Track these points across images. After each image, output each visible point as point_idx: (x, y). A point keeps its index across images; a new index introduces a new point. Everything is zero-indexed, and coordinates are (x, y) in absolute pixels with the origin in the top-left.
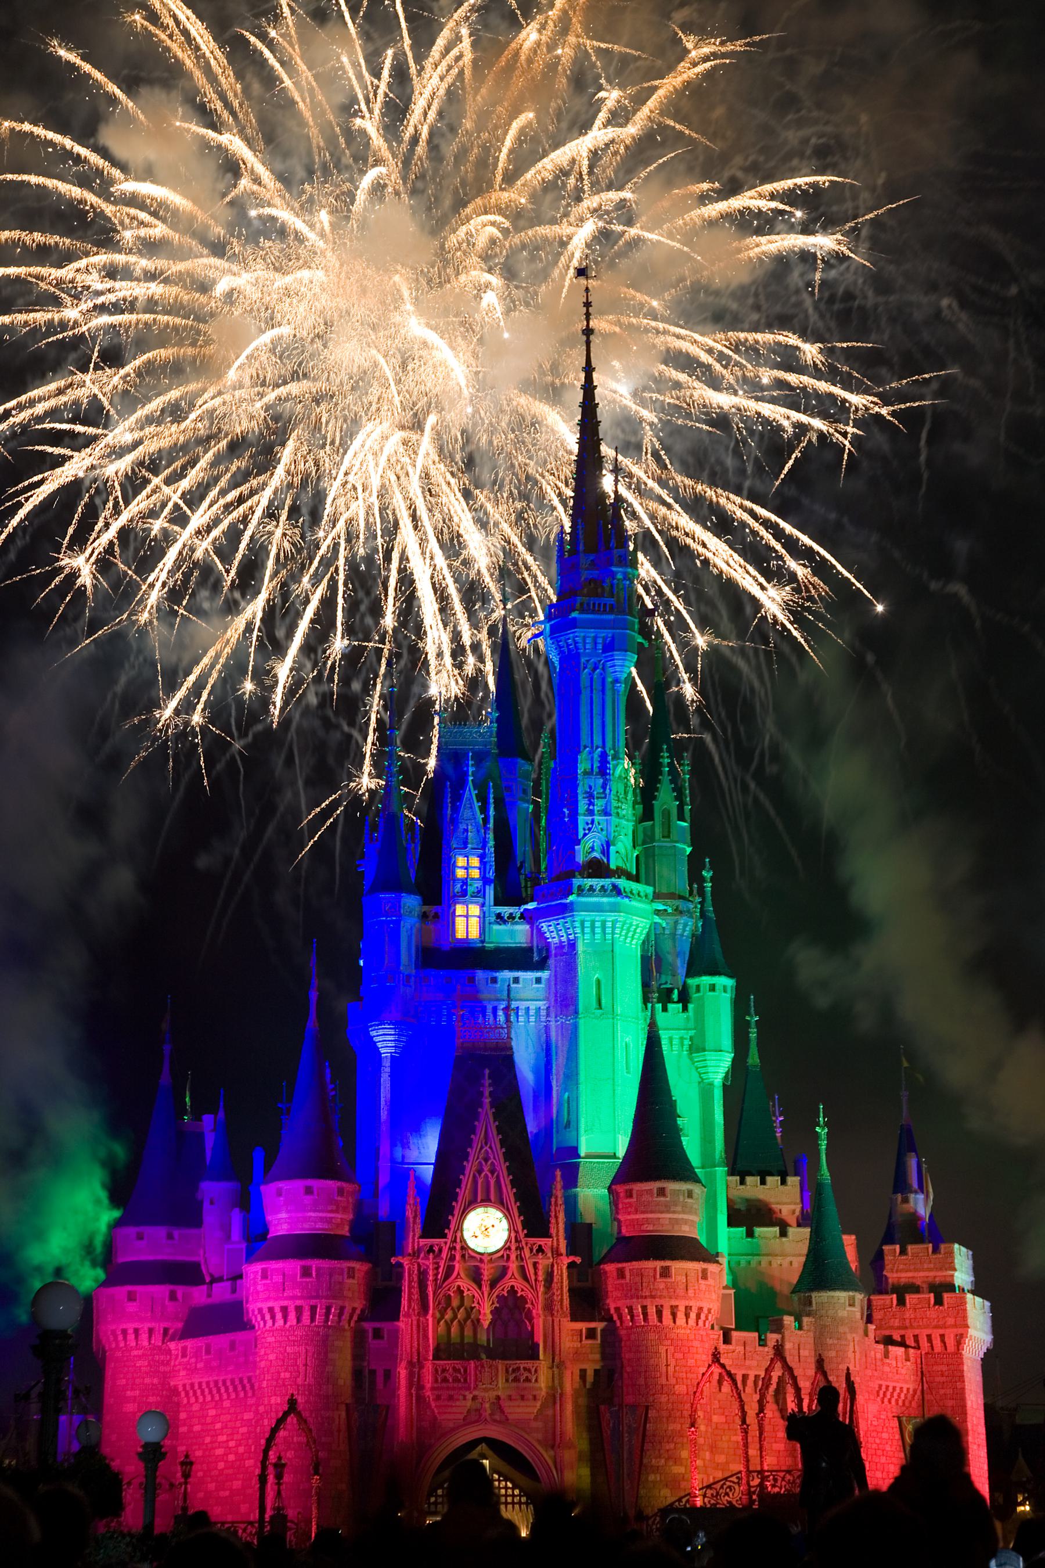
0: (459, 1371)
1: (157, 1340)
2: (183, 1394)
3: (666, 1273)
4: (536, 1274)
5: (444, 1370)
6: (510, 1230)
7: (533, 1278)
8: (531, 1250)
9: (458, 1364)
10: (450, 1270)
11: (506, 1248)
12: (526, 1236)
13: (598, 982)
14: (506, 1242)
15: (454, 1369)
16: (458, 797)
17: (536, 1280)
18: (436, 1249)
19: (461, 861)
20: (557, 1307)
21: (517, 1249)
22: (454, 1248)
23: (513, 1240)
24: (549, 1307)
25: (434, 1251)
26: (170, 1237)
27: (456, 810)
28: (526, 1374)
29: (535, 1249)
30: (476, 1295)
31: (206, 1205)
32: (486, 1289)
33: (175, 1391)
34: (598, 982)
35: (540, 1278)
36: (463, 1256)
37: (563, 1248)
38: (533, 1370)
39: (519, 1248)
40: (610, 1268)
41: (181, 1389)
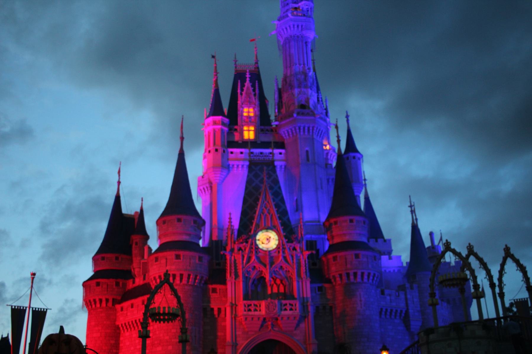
0: (257, 306)
1: (110, 304)
2: (121, 328)
3: (357, 256)
4: (293, 259)
5: (249, 306)
6: (279, 240)
7: (291, 262)
8: (290, 249)
9: (256, 302)
10: (249, 258)
11: (278, 247)
12: (287, 242)
13: (307, 151)
14: (278, 245)
15: (254, 305)
16: (243, 86)
17: (293, 262)
18: (243, 248)
19: (246, 110)
20: (303, 275)
21: (283, 248)
22: (252, 248)
23: (281, 244)
24: (299, 275)
25: (242, 250)
26: (117, 258)
27: (242, 90)
28: (290, 307)
29: (291, 248)
30: (264, 271)
31: (134, 246)
32: (268, 267)
33: (118, 328)
34: (307, 151)
35: (295, 262)
36: (256, 252)
37: (304, 247)
38: (294, 305)
39: (284, 248)
40: (330, 256)
41: (120, 326)
